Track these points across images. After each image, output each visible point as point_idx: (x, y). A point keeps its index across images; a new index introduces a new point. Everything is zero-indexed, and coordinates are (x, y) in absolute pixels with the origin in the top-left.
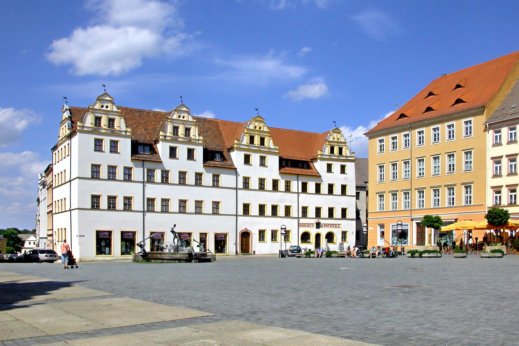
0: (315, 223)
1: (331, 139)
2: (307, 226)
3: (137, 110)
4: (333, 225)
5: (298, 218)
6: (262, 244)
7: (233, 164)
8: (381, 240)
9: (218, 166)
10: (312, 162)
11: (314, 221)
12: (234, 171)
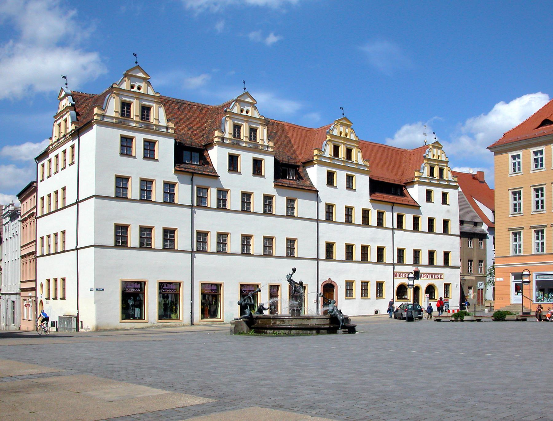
1: (430, 156)
2: (403, 276)
3: (175, 100)
4: (433, 275)
5: (393, 265)
7: (311, 185)
8: (516, 295)
9: (294, 186)
10: (405, 187)
11: (412, 269)
12: (313, 195)
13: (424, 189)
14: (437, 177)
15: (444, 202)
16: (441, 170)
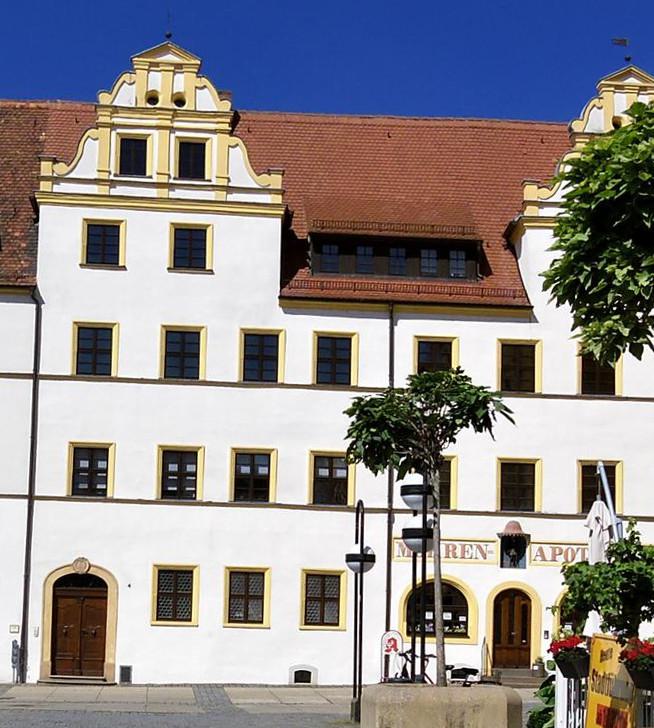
0: (499, 540)
6: (173, 631)
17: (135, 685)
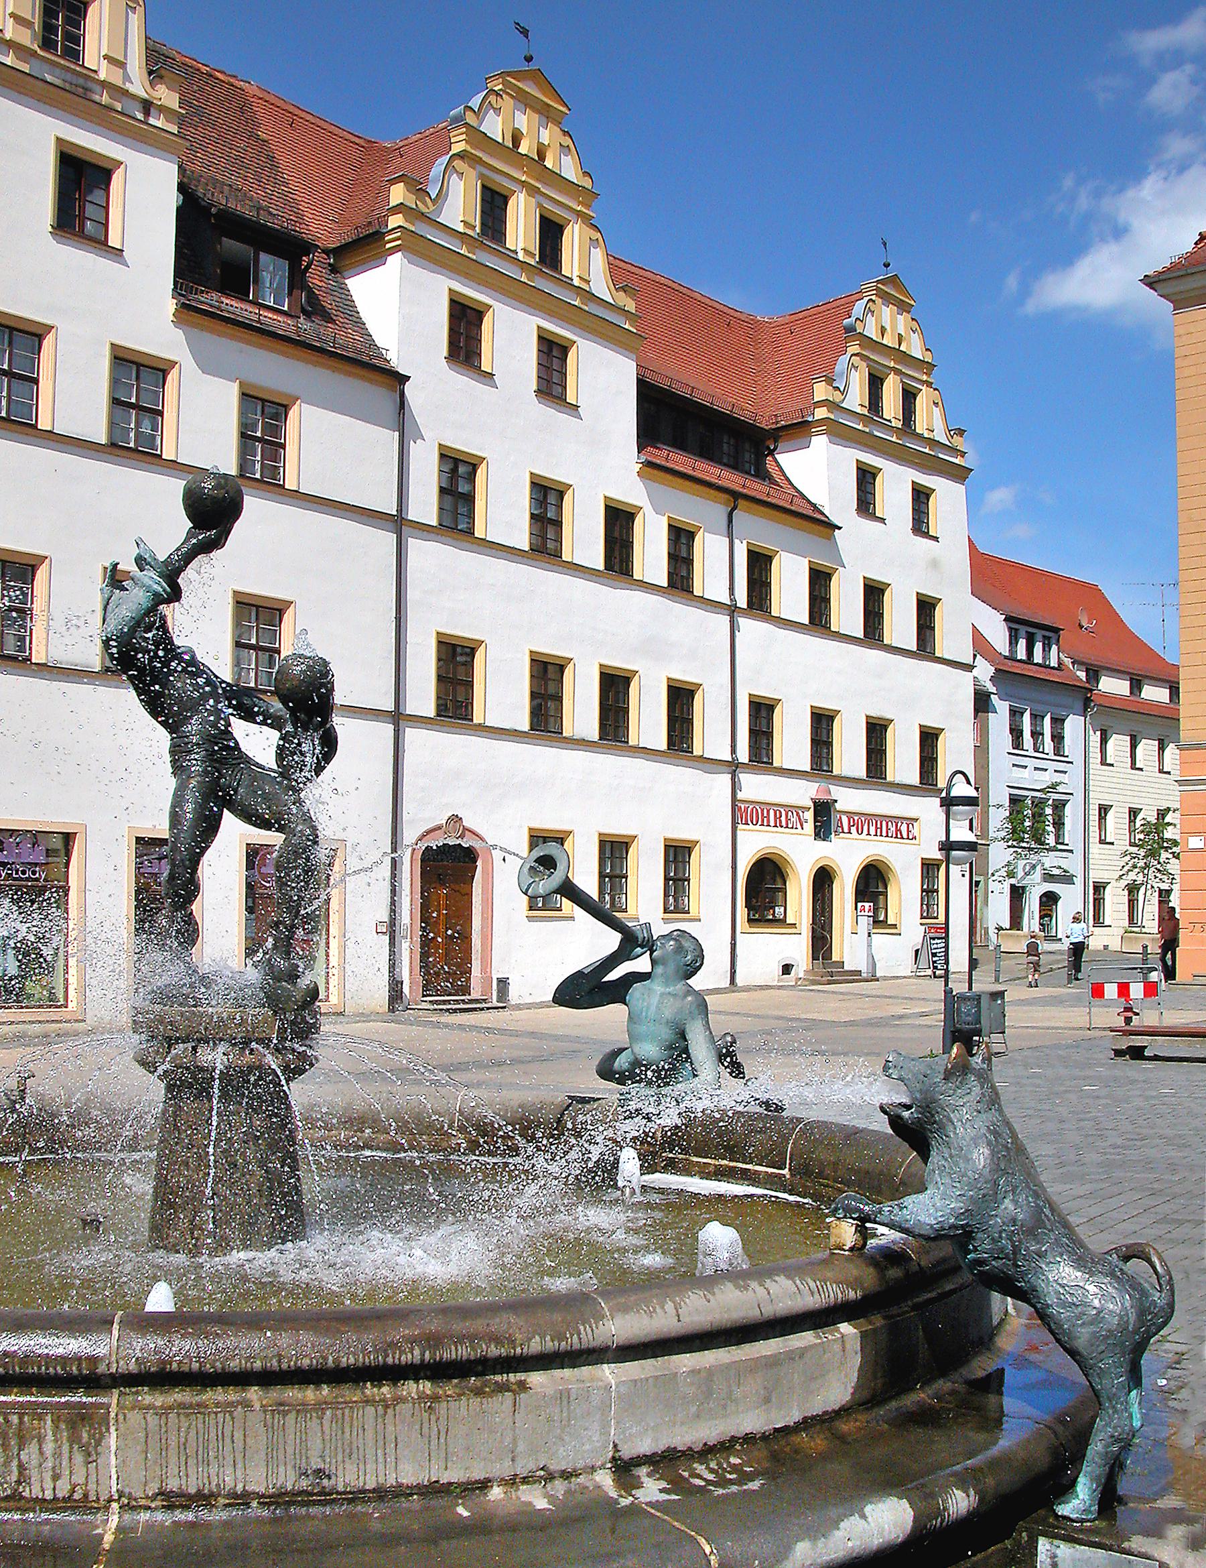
0: (812, 805)
1: (871, 331)
4: (884, 823)
5: (734, 767)
11: (803, 793)
13: (850, 457)
14: (893, 420)
15: (920, 525)
16: (909, 397)
17: (518, 1007)
